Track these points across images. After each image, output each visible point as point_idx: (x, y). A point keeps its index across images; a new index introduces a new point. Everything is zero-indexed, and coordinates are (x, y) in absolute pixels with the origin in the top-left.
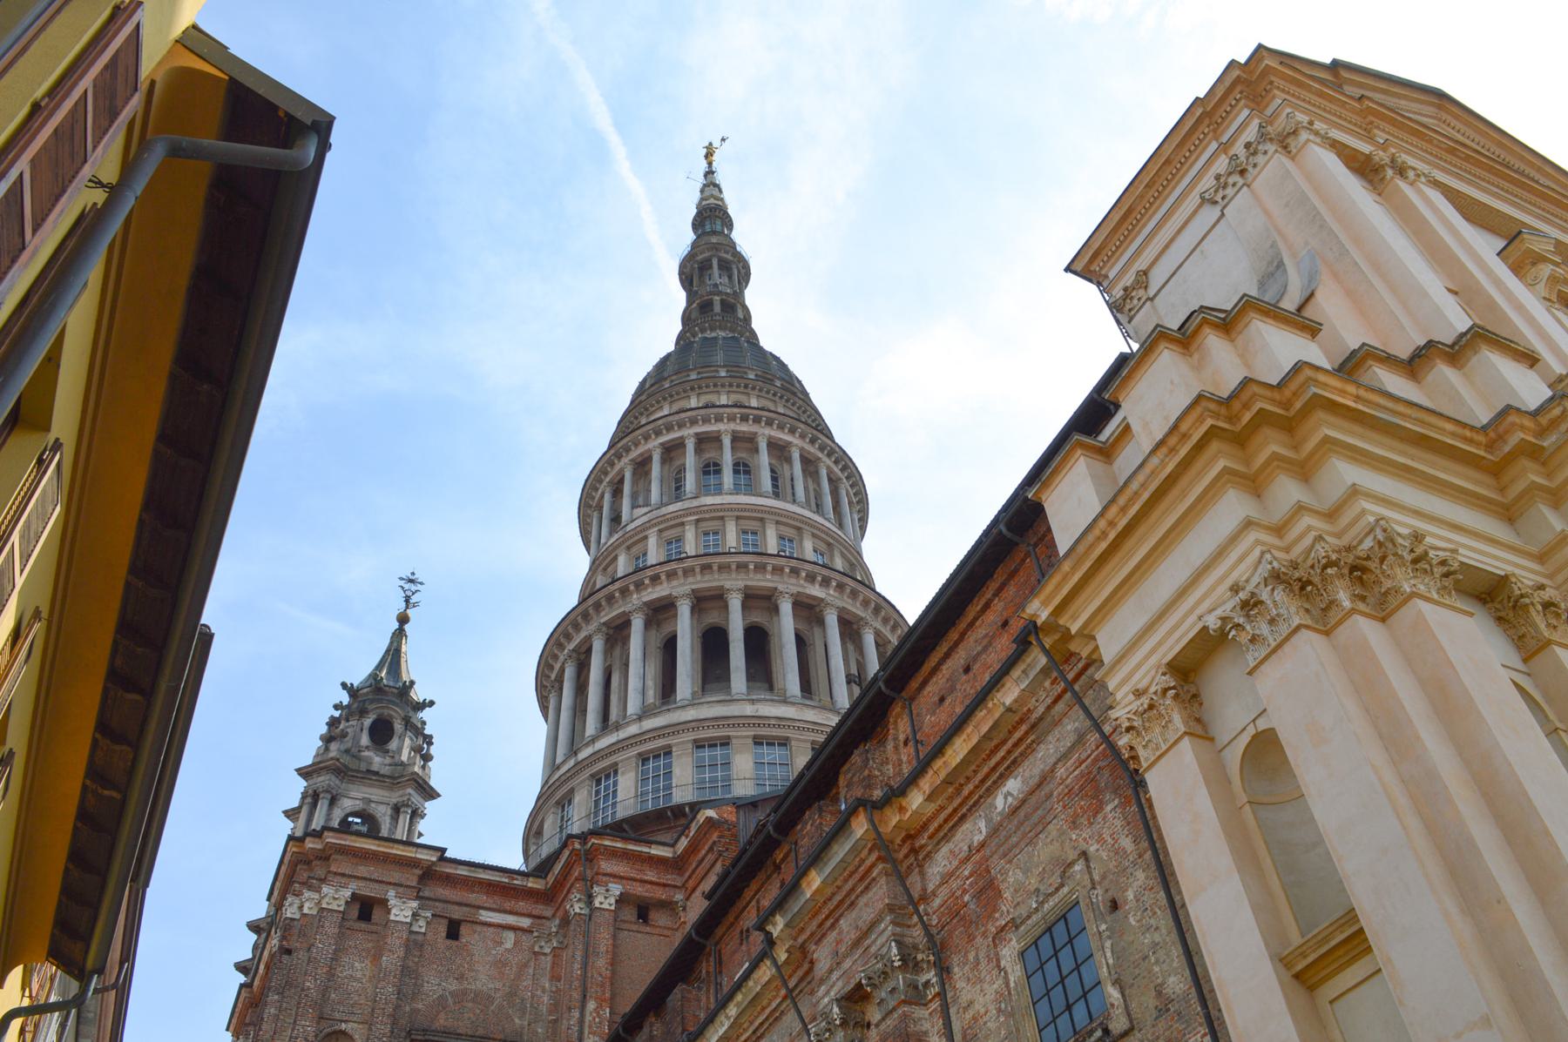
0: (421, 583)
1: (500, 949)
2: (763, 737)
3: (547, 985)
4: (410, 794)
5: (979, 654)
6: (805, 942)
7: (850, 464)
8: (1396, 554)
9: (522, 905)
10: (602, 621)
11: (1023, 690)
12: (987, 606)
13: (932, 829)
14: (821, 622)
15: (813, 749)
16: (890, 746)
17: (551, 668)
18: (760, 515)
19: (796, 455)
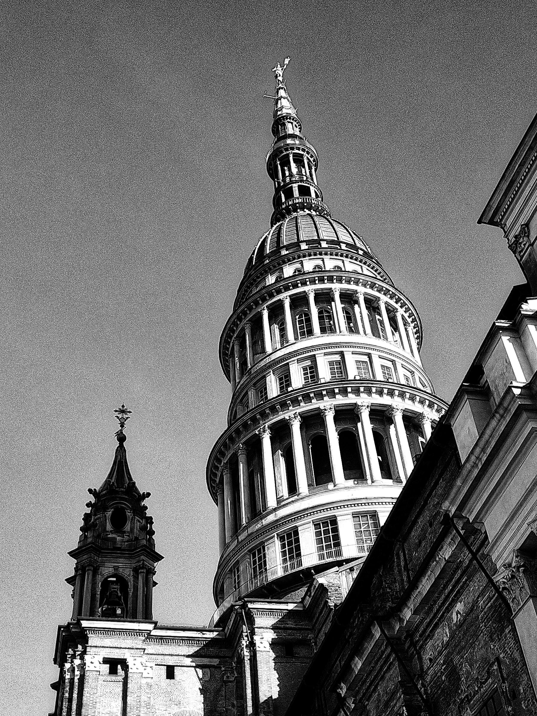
0: (130, 412)
2: (359, 513)
3: (235, 702)
4: (143, 560)
6: (361, 699)
12: (437, 483)
13: (422, 629)
17: (215, 475)
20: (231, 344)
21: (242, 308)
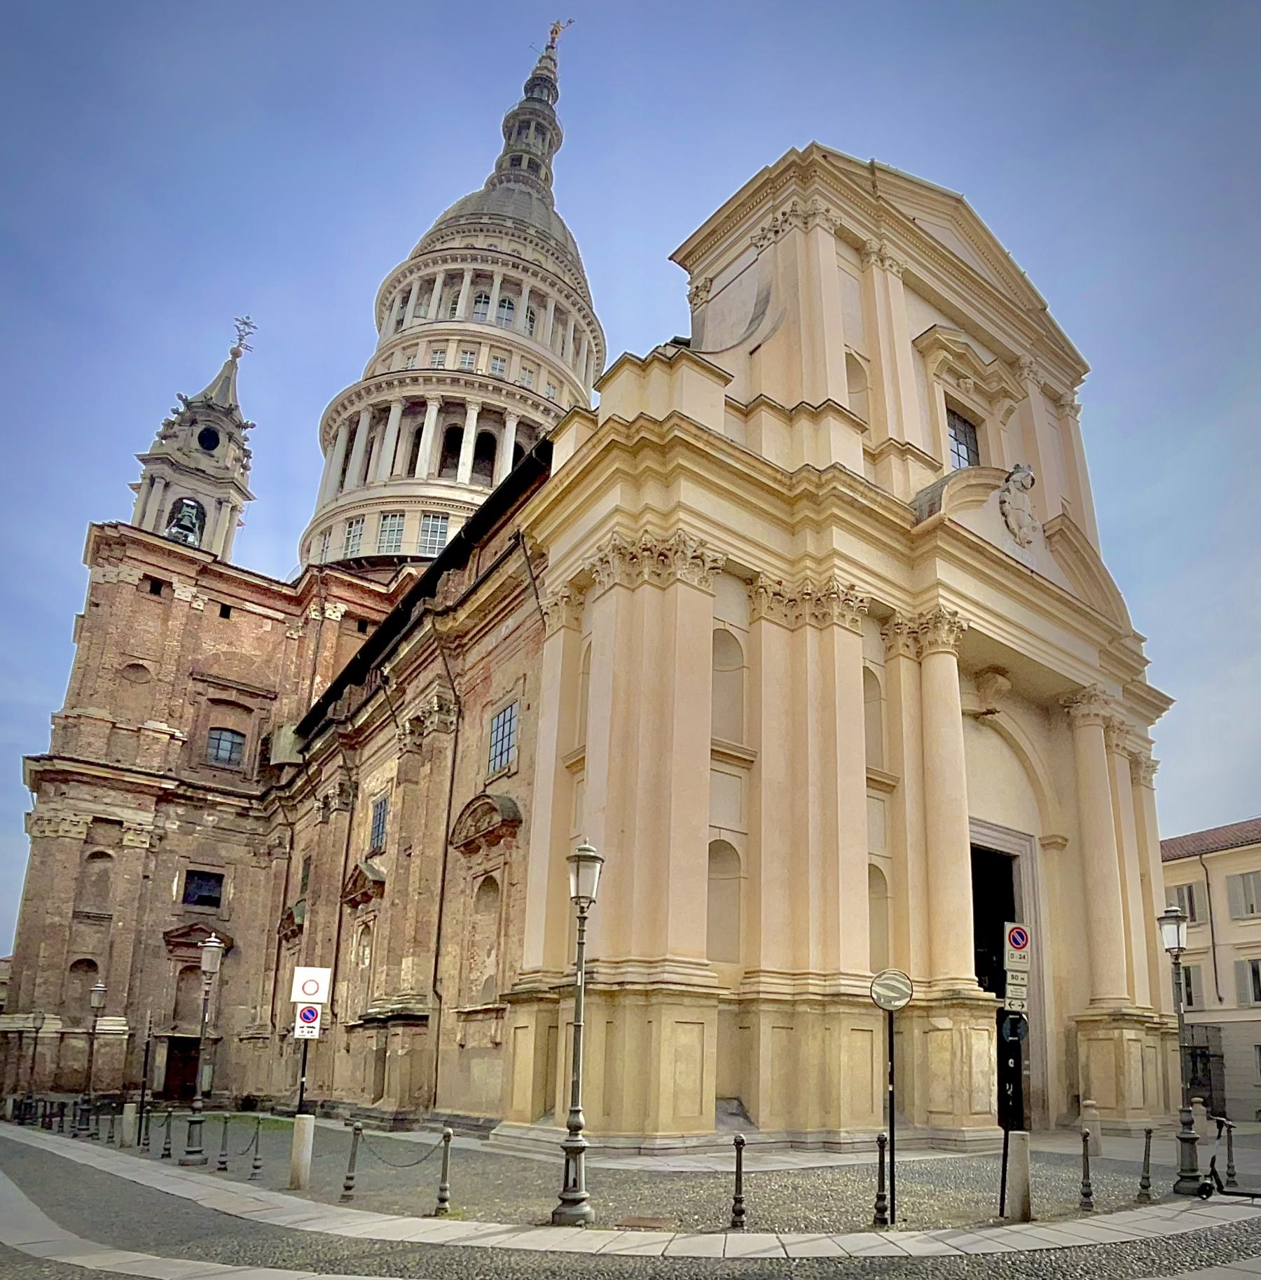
1: (261, 631)
8: (683, 552)
9: (279, 604)
18: (509, 348)
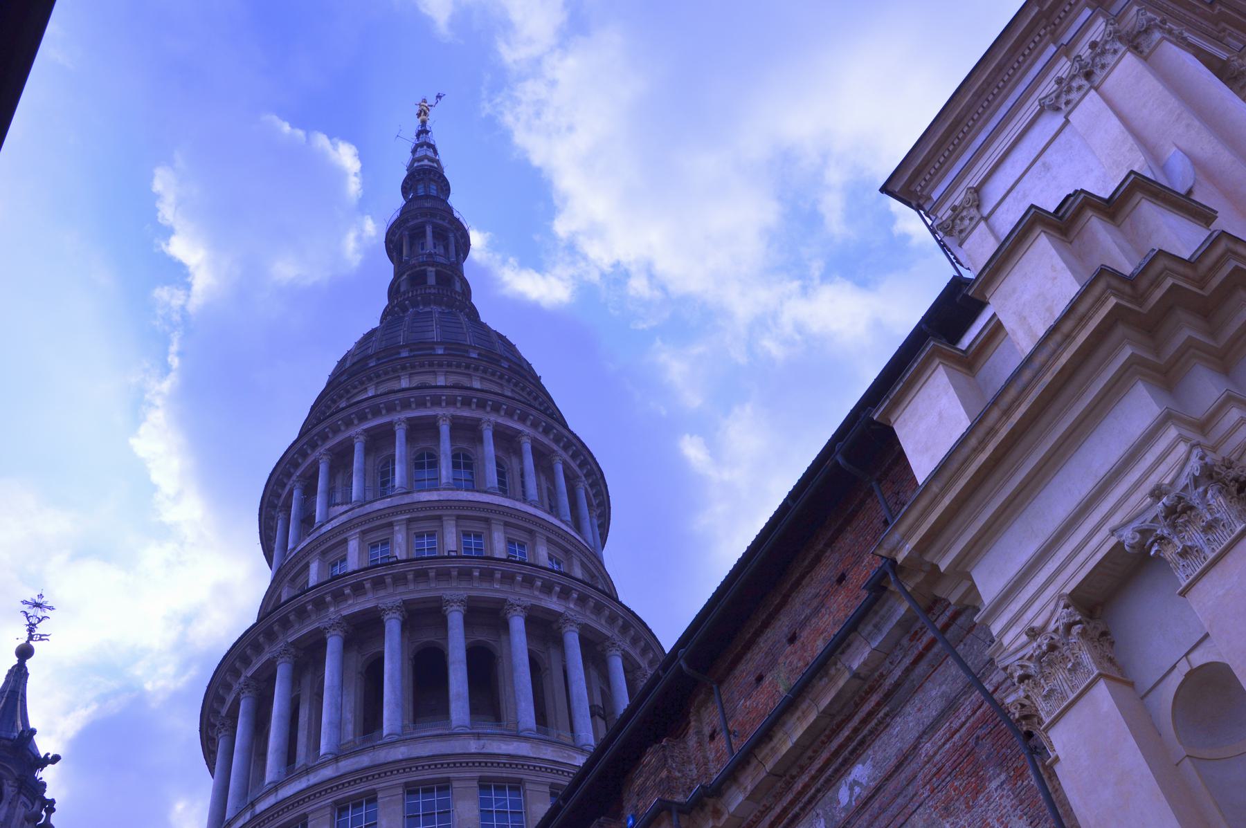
0: (51, 608)
2: (490, 779)
5: (808, 619)
7: (590, 460)
10: (290, 640)
11: (874, 649)
12: (817, 560)
14: (559, 642)
15: (552, 794)
16: (692, 741)
17: (222, 701)
18: (483, 514)
19: (527, 447)
20: (288, 488)
21: (320, 427)
